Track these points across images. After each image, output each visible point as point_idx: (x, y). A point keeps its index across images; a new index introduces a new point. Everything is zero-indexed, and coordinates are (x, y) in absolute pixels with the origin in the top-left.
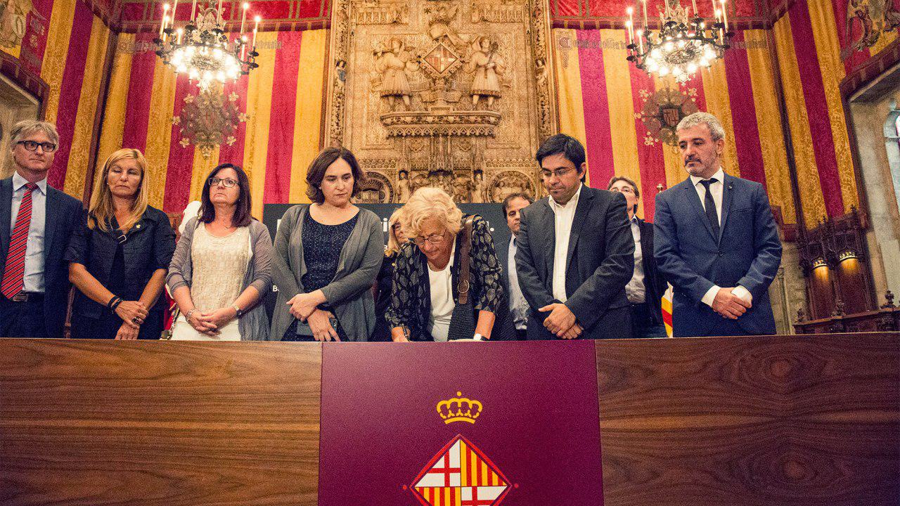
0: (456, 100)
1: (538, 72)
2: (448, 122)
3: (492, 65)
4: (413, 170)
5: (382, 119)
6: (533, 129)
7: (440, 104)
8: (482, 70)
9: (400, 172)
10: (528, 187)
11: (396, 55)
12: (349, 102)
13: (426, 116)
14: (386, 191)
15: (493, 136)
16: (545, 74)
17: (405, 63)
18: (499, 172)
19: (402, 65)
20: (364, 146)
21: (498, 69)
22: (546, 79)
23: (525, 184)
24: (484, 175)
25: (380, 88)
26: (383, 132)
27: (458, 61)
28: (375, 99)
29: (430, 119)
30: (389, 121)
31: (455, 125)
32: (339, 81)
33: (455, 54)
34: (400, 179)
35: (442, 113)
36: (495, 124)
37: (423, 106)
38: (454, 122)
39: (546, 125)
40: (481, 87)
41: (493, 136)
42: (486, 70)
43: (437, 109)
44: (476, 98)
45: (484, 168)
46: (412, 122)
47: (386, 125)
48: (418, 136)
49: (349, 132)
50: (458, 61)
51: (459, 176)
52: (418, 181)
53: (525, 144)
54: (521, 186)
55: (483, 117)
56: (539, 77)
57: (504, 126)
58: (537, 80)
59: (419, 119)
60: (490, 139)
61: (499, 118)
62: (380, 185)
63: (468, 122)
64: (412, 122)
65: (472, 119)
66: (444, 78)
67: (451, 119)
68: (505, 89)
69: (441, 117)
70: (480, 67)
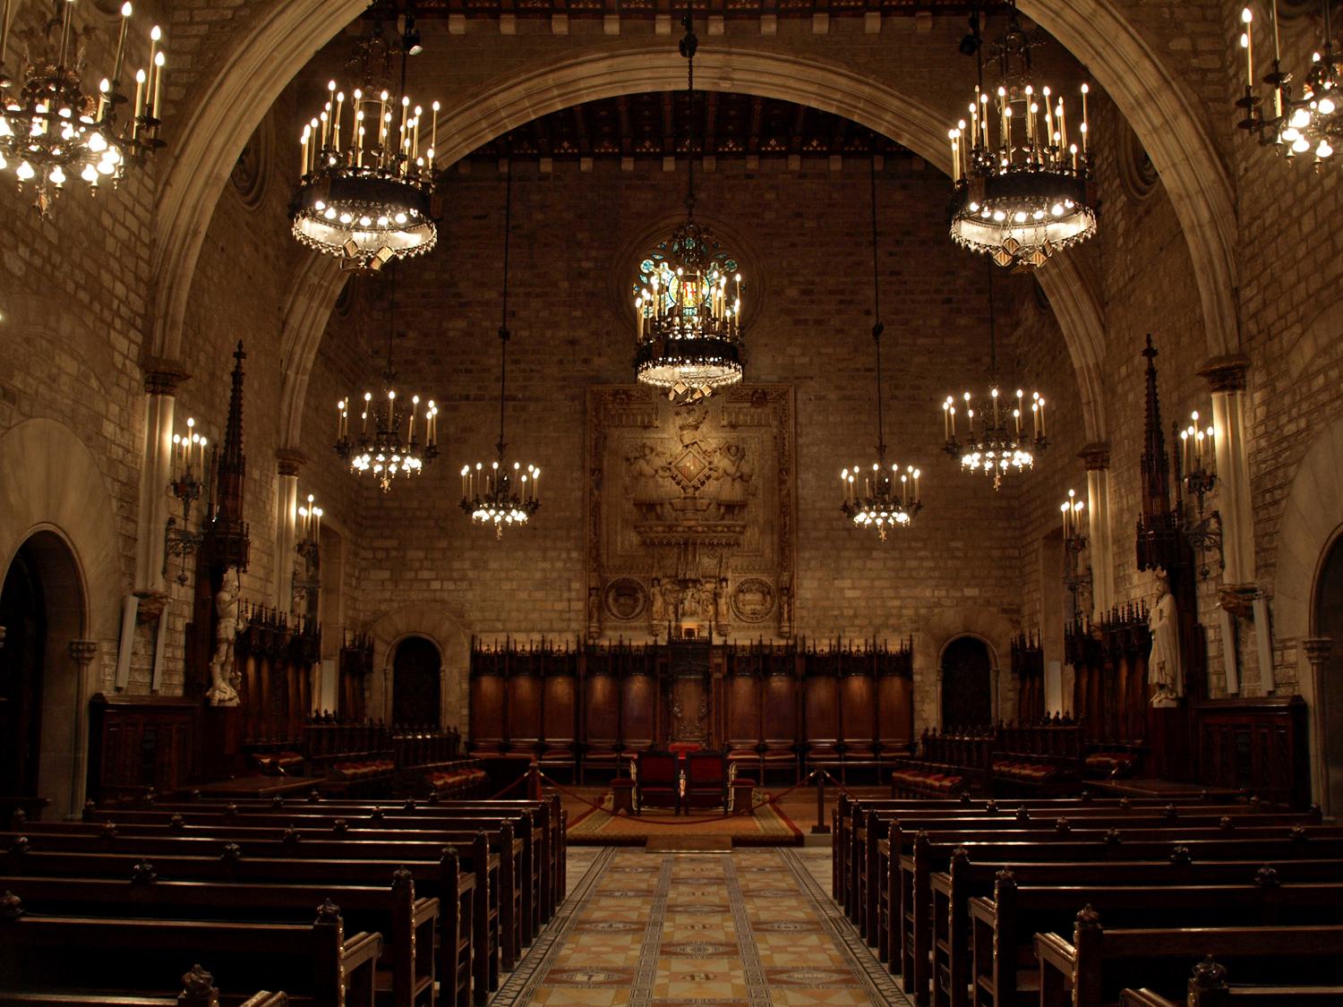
0: (705, 508)
1: (782, 482)
2: (697, 532)
3: (738, 474)
4: (665, 576)
5: (635, 527)
6: (776, 537)
7: (690, 515)
8: (730, 479)
9: (653, 580)
10: (769, 593)
11: (648, 463)
12: (604, 508)
13: (677, 526)
14: (640, 595)
15: (739, 545)
16: (788, 484)
17: (656, 471)
18: (743, 579)
19: (653, 472)
20: (619, 553)
21: (745, 477)
22: (789, 491)
23: (766, 590)
24: (729, 583)
25: (633, 495)
26: (635, 538)
27: (706, 469)
28: (629, 506)
29: (680, 529)
30: (642, 529)
31: (704, 535)
32: (596, 492)
33: (703, 461)
34: (653, 586)
35: (692, 523)
36: (741, 533)
37: (674, 514)
38: (703, 532)
39: (787, 536)
40: (728, 498)
41: (739, 545)
42: (733, 480)
43: (687, 520)
44: (722, 510)
45: (730, 575)
46: (664, 532)
47: (639, 533)
48: (669, 544)
49: (605, 539)
50: (706, 469)
51: (707, 582)
52: (669, 587)
53: (768, 551)
54: (763, 592)
55: (729, 527)
56: (783, 487)
57: (748, 534)
58: (780, 490)
59: (670, 528)
60: (735, 548)
61: (744, 527)
62: (635, 590)
63: (715, 532)
64: (664, 532)
65: (720, 529)
66: (694, 486)
67: (700, 529)
68: (751, 497)
69: (690, 528)
70: (728, 475)
